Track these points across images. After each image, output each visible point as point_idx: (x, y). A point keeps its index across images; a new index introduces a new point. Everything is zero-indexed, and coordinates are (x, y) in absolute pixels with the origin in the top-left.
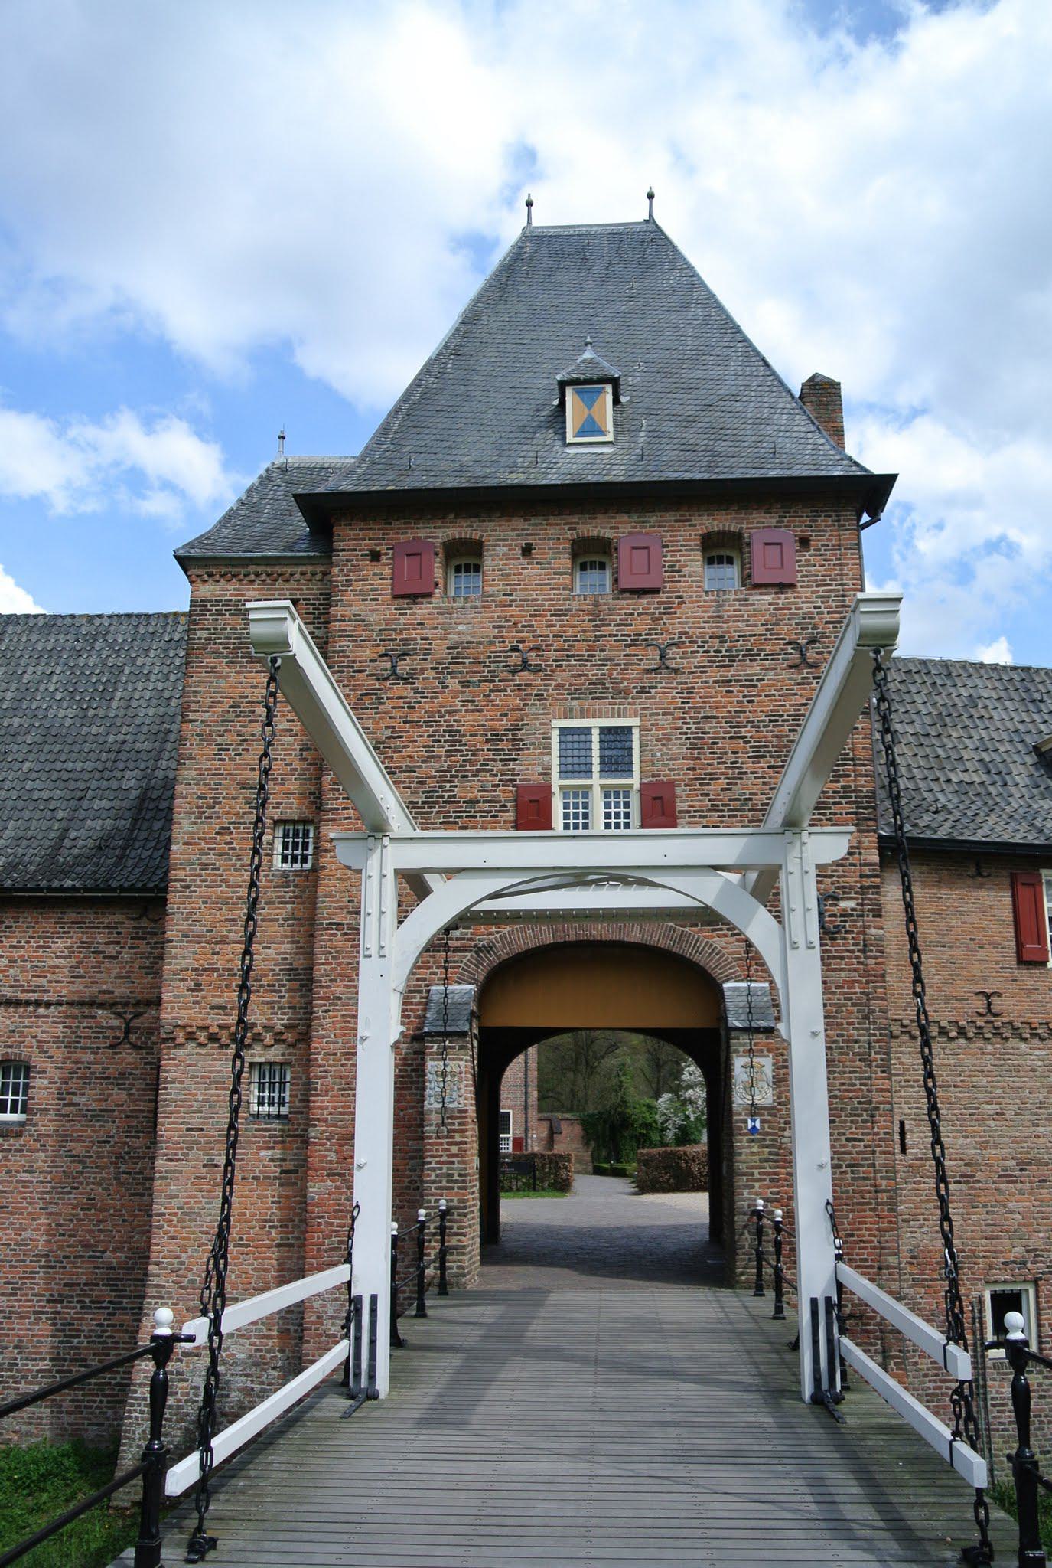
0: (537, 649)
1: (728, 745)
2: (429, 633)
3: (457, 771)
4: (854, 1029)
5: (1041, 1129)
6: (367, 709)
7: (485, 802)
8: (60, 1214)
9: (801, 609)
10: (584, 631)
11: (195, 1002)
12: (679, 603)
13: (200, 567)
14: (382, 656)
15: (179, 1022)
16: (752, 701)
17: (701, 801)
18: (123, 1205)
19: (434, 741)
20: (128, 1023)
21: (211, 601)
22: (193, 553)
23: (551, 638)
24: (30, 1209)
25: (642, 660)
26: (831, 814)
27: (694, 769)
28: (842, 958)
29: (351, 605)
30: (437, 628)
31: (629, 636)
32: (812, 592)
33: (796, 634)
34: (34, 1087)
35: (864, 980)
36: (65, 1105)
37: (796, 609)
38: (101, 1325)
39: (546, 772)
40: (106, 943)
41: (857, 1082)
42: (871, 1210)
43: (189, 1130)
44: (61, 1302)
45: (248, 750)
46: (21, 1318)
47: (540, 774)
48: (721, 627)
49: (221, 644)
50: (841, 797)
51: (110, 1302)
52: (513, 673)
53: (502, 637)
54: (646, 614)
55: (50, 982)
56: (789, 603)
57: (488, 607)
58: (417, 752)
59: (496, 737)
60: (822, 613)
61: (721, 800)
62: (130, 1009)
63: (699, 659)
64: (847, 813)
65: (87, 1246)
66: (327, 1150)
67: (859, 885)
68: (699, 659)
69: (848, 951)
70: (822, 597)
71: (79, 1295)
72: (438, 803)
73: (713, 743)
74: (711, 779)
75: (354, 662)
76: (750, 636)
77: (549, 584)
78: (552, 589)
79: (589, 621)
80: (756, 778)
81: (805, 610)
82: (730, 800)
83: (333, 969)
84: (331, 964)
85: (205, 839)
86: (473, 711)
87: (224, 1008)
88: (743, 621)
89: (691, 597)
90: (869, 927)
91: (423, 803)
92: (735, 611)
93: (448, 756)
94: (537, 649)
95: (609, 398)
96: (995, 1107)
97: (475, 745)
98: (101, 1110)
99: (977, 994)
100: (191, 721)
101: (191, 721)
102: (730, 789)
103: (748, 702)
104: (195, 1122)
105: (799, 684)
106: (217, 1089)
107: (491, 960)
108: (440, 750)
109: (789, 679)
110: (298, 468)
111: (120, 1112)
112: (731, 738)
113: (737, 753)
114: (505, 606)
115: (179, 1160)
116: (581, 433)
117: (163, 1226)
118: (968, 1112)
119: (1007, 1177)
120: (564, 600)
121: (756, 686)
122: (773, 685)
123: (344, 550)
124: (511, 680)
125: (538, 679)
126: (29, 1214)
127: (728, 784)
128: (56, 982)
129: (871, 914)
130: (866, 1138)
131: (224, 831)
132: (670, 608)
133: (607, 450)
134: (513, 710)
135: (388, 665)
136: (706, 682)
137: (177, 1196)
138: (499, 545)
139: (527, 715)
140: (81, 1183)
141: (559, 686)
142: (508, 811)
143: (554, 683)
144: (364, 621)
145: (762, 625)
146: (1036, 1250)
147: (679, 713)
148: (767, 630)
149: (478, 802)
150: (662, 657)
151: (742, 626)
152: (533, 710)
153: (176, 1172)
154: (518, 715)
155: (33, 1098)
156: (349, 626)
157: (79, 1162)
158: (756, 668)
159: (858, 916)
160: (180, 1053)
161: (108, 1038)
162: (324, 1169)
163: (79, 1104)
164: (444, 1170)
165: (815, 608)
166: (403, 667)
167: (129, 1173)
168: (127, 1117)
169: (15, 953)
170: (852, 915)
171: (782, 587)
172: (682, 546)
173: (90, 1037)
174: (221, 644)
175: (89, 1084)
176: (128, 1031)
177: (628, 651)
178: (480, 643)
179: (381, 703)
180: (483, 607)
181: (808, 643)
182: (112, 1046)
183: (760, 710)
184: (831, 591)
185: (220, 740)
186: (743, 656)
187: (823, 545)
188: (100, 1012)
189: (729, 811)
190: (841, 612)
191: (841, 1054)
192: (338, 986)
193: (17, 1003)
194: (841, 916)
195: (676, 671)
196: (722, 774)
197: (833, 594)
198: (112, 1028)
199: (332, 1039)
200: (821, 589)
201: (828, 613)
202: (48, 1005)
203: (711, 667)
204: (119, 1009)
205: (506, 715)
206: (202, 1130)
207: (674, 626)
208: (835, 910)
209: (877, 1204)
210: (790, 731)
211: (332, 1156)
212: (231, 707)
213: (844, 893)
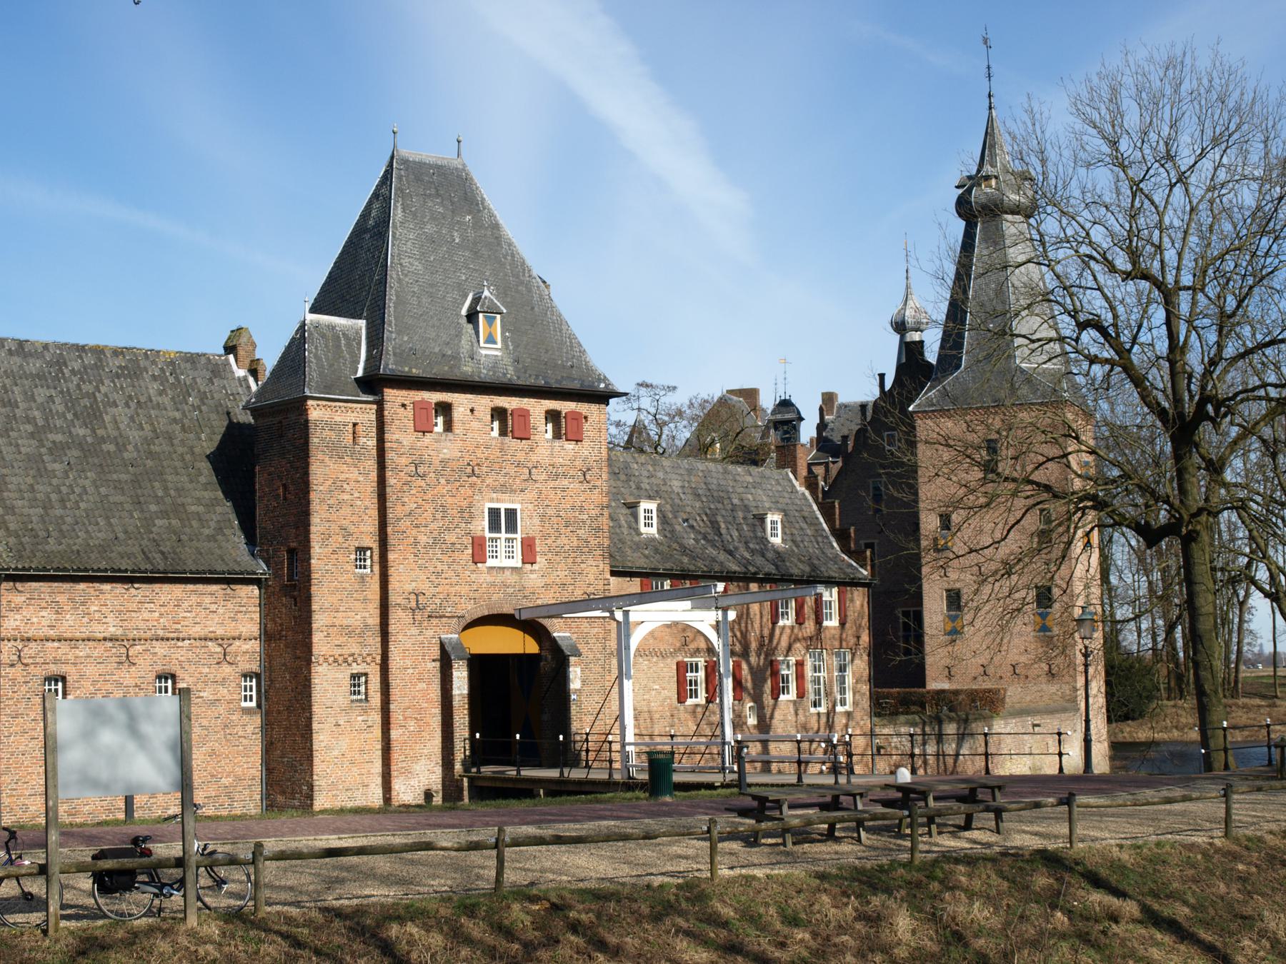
0: (478, 465)
2: (431, 453)
58: (428, 515)
63: (544, 476)
68: (544, 476)
94: (478, 465)
104: (329, 704)
107: (464, 623)
108: (439, 516)
116: (487, 342)
131: (334, 552)
141: (488, 485)
147: (536, 503)
151: (561, 460)
154: (471, 500)
156: (395, 446)
158: (565, 482)
160: (319, 669)
166: (421, 470)
169: (162, 610)
176: (225, 655)
182: (218, 663)
193: (168, 639)
207: (534, 458)
211: (401, 717)
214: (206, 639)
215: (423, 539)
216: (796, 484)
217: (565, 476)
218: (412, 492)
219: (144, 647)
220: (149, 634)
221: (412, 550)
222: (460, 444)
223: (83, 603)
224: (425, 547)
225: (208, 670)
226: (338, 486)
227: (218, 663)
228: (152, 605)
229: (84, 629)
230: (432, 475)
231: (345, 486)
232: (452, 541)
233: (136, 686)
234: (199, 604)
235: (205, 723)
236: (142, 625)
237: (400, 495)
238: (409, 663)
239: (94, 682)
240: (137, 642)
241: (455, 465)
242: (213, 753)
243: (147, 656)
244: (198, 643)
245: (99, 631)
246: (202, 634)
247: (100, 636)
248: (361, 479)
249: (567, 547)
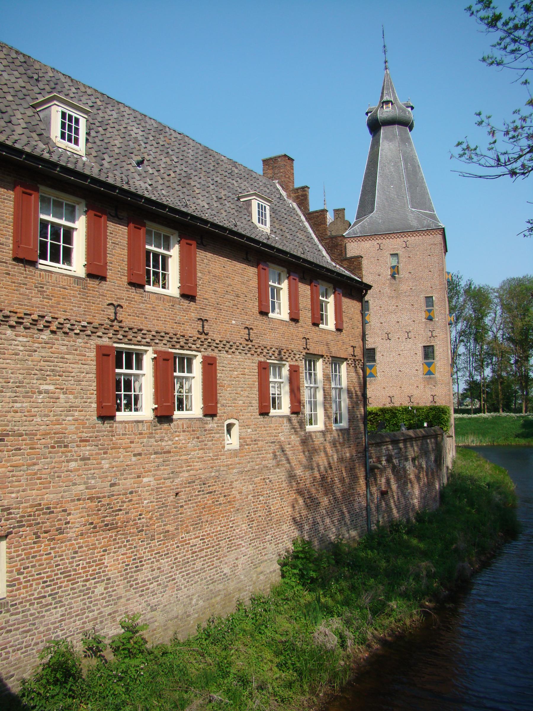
5: (19, 405)
146: (9, 509)
216: (284, 193)
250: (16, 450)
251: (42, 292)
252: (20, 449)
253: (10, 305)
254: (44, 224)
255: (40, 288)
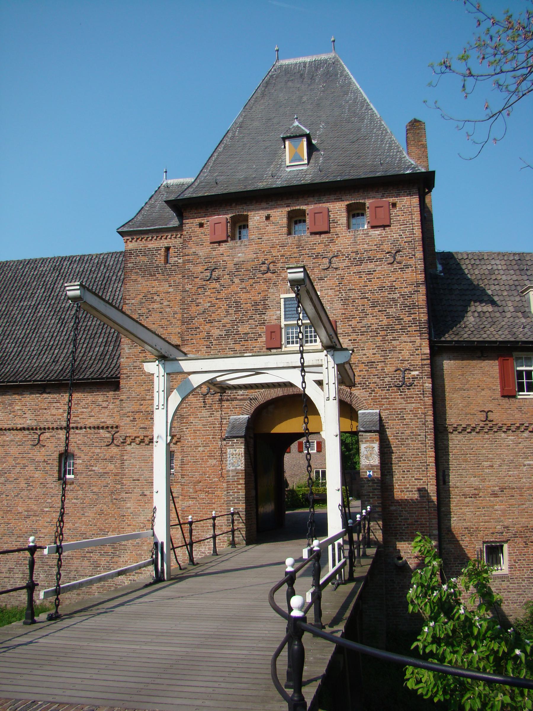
1: (360, 302)
2: (225, 258)
3: (239, 320)
4: (418, 430)
5: (512, 473)
6: (200, 294)
7: (252, 333)
8: (89, 516)
9: (393, 236)
10: (294, 253)
11: (134, 426)
12: (337, 237)
13: (128, 236)
14: (206, 270)
15: (128, 435)
16: (371, 281)
17: (347, 328)
18: (115, 513)
19: (229, 307)
20: (113, 435)
21: (133, 250)
22: (125, 229)
23: (280, 257)
24: (78, 515)
25: (320, 265)
26: (407, 331)
27: (344, 314)
28: (413, 398)
29: (192, 248)
30: (229, 256)
31: (314, 254)
32: (398, 228)
33: (391, 248)
34: (76, 464)
35: (423, 407)
36: (90, 471)
37: (391, 237)
38: (109, 562)
39: (279, 318)
40: (103, 401)
41: (419, 454)
42: (426, 510)
43: (133, 480)
44: (92, 553)
45: (151, 315)
46: (77, 559)
47: (276, 320)
48: (356, 247)
49: (138, 269)
50: (412, 324)
51: (112, 553)
52: (263, 274)
53: (258, 258)
54: (322, 243)
55: (80, 419)
56: (387, 234)
57: (251, 245)
58: (222, 312)
59: (256, 304)
60: (403, 238)
61: (357, 327)
62: (115, 429)
63: (347, 263)
64: (415, 331)
65: (101, 530)
66: (189, 488)
67: (420, 364)
68: (347, 263)
69: (416, 394)
70: (403, 230)
71: (99, 550)
72: (231, 335)
73: (353, 301)
74: (352, 318)
75: (194, 273)
76: (370, 250)
77: (278, 232)
78: (279, 235)
79: (297, 248)
80: (373, 316)
81: (395, 237)
82: (361, 327)
83: (189, 410)
84: (188, 408)
85: (135, 355)
86: (246, 292)
87: (146, 428)
88: (366, 244)
89: (342, 234)
90: (425, 383)
91: (225, 335)
92: (362, 239)
93: (235, 314)
95: (305, 144)
96: (489, 463)
97: (247, 308)
98: (104, 473)
99: (481, 411)
100: (127, 304)
101: (127, 304)
102: (361, 322)
103: (369, 281)
104: (136, 477)
105: (392, 272)
106: (144, 463)
107: (256, 405)
109: (388, 270)
110: (173, 185)
111: (112, 473)
112: (361, 298)
113: (364, 305)
114: (259, 244)
115: (130, 493)
117: (125, 521)
118: (476, 465)
119: (495, 495)
120: (285, 239)
121: (373, 274)
122: (380, 273)
123: (188, 223)
124: (262, 278)
125: (274, 276)
126: (78, 516)
127: (360, 320)
128: (83, 419)
129: (426, 377)
130: (424, 478)
132: (333, 240)
133: (305, 168)
134: (263, 291)
135: (209, 274)
136: (350, 273)
137: (130, 508)
138: (255, 216)
139: (269, 293)
140: (97, 503)
142: (262, 337)
143: (281, 278)
144: (197, 255)
145: (375, 245)
146: (508, 527)
148: (377, 247)
149: (249, 333)
150: (330, 262)
152: (272, 291)
153: (129, 498)
155: (76, 468)
157: (96, 495)
158: (371, 266)
159: (420, 378)
160: (128, 448)
161: (105, 442)
162: (188, 495)
163: (94, 471)
164: (236, 496)
165: (399, 236)
167: (117, 499)
168: (115, 475)
170: (417, 378)
171: (384, 227)
172: (338, 210)
173: (98, 442)
174: (138, 269)
175: (98, 462)
176: (113, 439)
177: (314, 261)
178: (248, 261)
179: (205, 291)
180: (249, 245)
181: (396, 253)
182: (107, 446)
183: (375, 284)
184: (407, 227)
185: (139, 311)
186: (367, 260)
187: (403, 206)
188: (101, 431)
189: (361, 332)
190: (412, 237)
191: (412, 441)
192: (191, 418)
194: (412, 378)
195: (336, 269)
196: (358, 315)
197: (407, 229)
198: (106, 438)
199: (190, 440)
200: (402, 227)
201: (405, 238)
202: (81, 428)
203: (352, 266)
204: (110, 429)
205: (260, 293)
206: (139, 480)
207: (334, 248)
208: (410, 376)
209: (429, 507)
210: (388, 294)
211: (191, 490)
212: (144, 297)
213: (413, 368)
214: (98, 428)
215: (216, 332)
217: (370, 260)
218: (206, 294)
219: (51, 434)
220: (55, 425)
221: (205, 343)
222: (255, 247)
223: (10, 405)
224: (217, 338)
225: (99, 451)
226: (149, 298)
227: (107, 446)
228: (58, 404)
229: (9, 422)
230: (226, 277)
231: (155, 297)
232: (246, 331)
233: (45, 461)
234: (93, 402)
235: (95, 489)
236: (50, 418)
237: (194, 297)
238: (199, 441)
239: (15, 459)
240: (47, 431)
241: (249, 266)
242: (101, 513)
243: (53, 440)
244: (92, 431)
245: (20, 423)
246: (96, 424)
247: (19, 426)
248: (171, 290)
249: (374, 327)
250: (511, 496)
251: (521, 411)
252: (513, 496)
253: (502, 421)
254: (520, 373)
255: (520, 409)
